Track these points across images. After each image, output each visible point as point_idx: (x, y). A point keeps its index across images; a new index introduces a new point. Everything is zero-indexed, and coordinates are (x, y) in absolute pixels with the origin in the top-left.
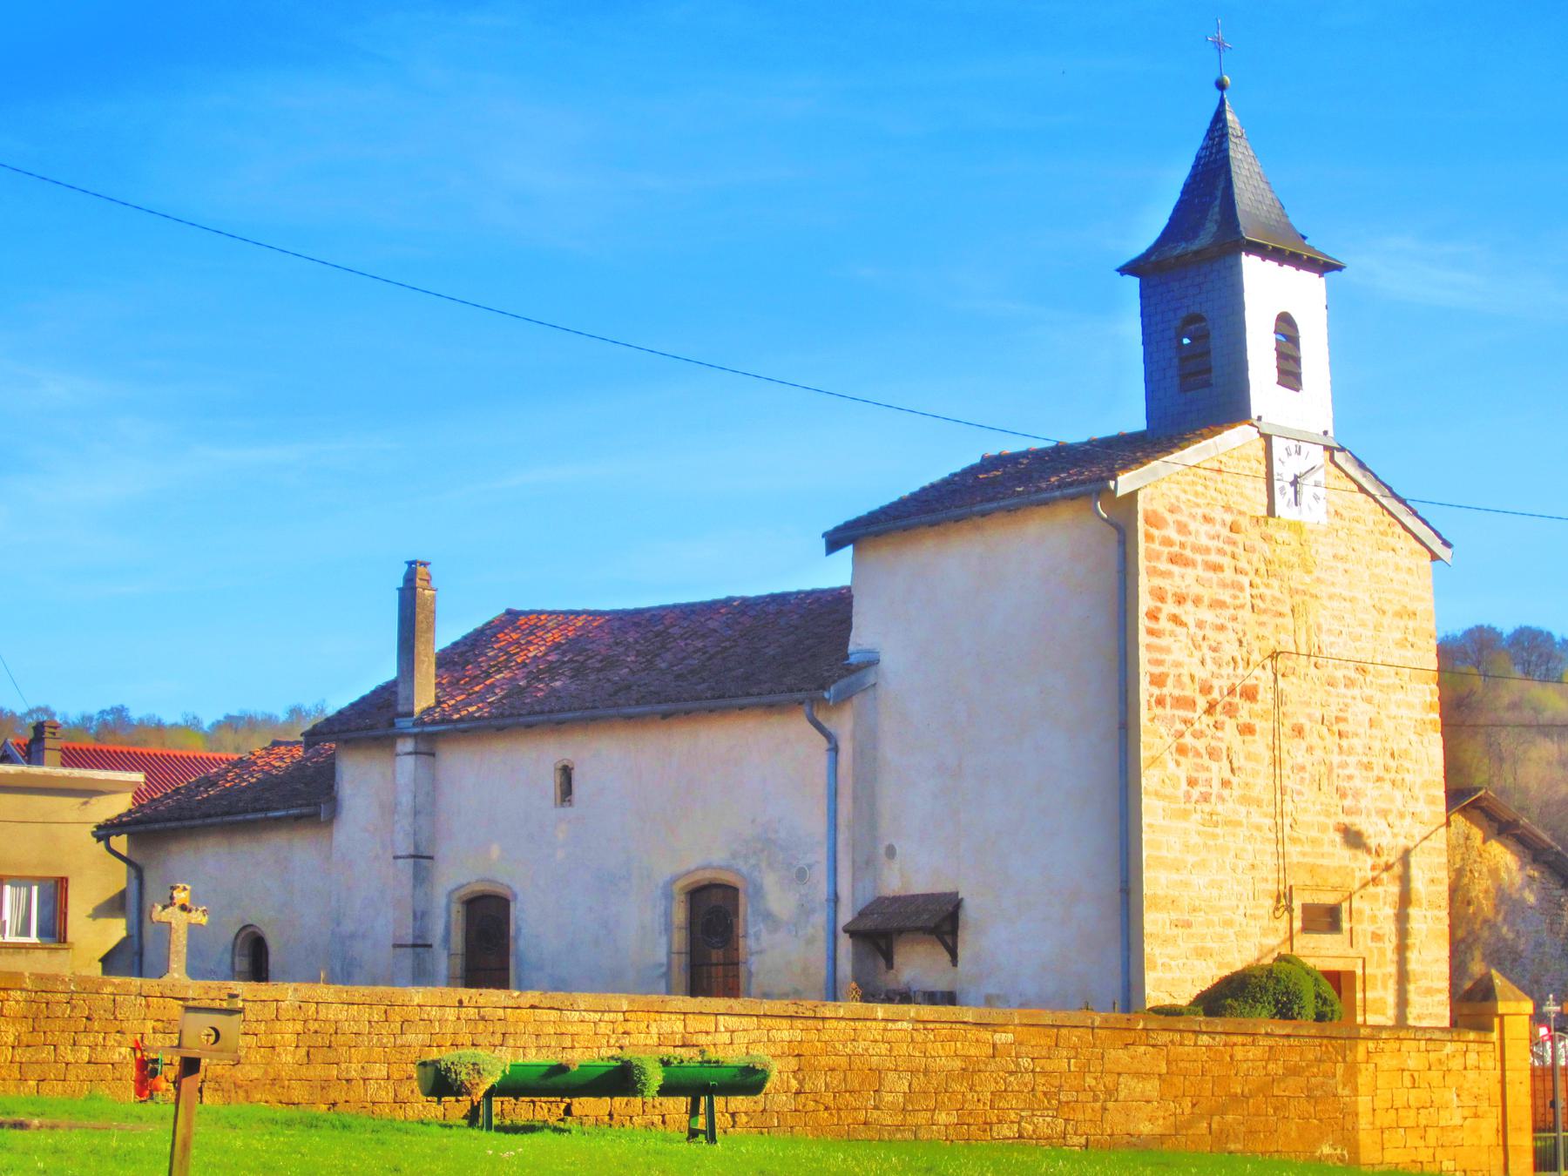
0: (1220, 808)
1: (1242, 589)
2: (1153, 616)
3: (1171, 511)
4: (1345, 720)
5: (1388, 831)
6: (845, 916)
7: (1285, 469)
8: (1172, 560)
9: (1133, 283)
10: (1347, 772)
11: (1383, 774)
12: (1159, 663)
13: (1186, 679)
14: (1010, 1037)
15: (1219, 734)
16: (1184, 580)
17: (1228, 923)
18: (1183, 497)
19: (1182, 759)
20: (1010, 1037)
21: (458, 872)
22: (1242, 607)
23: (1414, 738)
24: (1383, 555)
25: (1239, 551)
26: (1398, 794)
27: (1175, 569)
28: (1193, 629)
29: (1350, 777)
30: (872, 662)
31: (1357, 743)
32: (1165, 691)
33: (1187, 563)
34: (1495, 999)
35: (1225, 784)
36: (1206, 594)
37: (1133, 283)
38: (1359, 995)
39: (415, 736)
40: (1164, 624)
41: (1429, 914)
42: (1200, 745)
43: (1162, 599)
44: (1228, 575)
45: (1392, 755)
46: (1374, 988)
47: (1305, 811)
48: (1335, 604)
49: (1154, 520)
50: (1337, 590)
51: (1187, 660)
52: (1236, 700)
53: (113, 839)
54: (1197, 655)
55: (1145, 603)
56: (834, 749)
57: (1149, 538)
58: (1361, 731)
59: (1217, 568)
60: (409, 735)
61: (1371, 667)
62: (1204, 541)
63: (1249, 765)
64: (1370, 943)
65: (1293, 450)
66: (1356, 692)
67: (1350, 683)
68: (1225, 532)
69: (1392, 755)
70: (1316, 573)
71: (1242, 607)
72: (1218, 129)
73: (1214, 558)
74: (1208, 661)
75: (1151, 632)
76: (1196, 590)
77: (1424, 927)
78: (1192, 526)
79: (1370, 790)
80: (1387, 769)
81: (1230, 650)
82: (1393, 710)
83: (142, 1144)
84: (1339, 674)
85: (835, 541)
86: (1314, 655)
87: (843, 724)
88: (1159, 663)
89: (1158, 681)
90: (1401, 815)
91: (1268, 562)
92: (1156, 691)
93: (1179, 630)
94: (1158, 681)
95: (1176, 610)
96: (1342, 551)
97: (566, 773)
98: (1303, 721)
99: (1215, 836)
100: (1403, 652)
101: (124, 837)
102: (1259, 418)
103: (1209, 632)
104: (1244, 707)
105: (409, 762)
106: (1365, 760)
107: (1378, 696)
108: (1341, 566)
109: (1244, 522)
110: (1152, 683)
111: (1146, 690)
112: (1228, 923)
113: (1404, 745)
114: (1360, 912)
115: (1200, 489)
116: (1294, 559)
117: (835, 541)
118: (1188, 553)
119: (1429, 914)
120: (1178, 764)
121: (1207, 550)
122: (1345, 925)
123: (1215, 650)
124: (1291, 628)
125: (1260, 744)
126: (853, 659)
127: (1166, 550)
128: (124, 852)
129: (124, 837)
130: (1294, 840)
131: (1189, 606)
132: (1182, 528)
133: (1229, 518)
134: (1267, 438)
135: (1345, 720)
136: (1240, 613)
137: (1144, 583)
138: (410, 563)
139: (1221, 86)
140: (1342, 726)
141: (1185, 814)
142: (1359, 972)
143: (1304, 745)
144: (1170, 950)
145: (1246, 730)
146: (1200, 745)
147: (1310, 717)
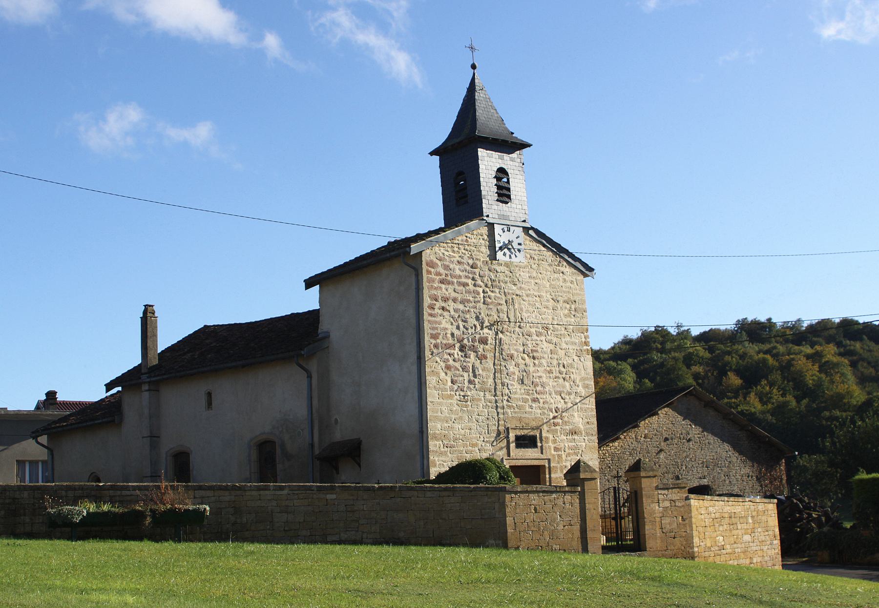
0: (469, 393)
1: (478, 294)
2: (432, 307)
3: (440, 260)
4: (536, 351)
5: (562, 401)
6: (317, 452)
7: (501, 238)
8: (442, 282)
9: (436, 158)
10: (539, 374)
11: (558, 375)
12: (433, 329)
13: (449, 336)
14: (334, 496)
15: (468, 359)
16: (447, 291)
17: (473, 445)
18: (446, 253)
19: (448, 372)
20: (334, 496)
21: (168, 444)
22: (479, 302)
23: (576, 358)
24: (556, 275)
25: (477, 277)
26: (567, 384)
27: (443, 286)
28: (452, 313)
29: (540, 377)
30: (327, 336)
31: (544, 361)
32: (439, 341)
33: (449, 283)
34: (579, 472)
35: (470, 382)
36: (459, 297)
37: (436, 158)
38: (547, 476)
39: (149, 382)
40: (437, 311)
41: (586, 438)
42: (457, 365)
43: (436, 300)
44: (471, 287)
45: (564, 366)
46: (556, 472)
47: (516, 393)
48: (530, 299)
49: (431, 264)
50: (532, 292)
51: (450, 327)
52: (476, 344)
53: (39, 439)
54: (455, 324)
55: (427, 301)
56: (310, 377)
57: (429, 272)
58: (546, 356)
59: (465, 285)
60: (145, 383)
61: (551, 326)
62: (458, 272)
63: (484, 374)
64: (553, 452)
65: (506, 229)
66: (543, 338)
67: (539, 334)
68: (468, 268)
69: (564, 366)
70: (519, 285)
71: (479, 302)
72: (472, 88)
73: (463, 280)
74: (461, 327)
75: (431, 315)
76: (454, 295)
77: (584, 444)
78: (451, 266)
79: (551, 382)
80: (560, 373)
81: (472, 321)
82: (564, 346)
83: (58, 583)
84: (533, 330)
85: (309, 283)
86: (520, 323)
87: (313, 366)
88: (433, 329)
89: (435, 337)
90: (570, 394)
91: (493, 281)
92: (433, 341)
93: (445, 313)
94: (435, 337)
95: (443, 304)
96: (534, 274)
97: (209, 395)
98: (512, 352)
99: (466, 406)
100: (568, 319)
101: (45, 437)
102: (488, 216)
103: (461, 314)
104: (480, 348)
105: (146, 394)
106: (548, 369)
107: (555, 340)
108: (533, 281)
109: (479, 264)
110: (431, 338)
111: (428, 342)
112: (473, 445)
113: (570, 361)
114: (547, 438)
115: (456, 249)
116: (507, 279)
117: (309, 283)
118: (449, 278)
119: (586, 438)
120: (446, 374)
121: (460, 277)
122: (539, 444)
123: (465, 322)
124: (505, 310)
125: (489, 364)
126: (320, 336)
127: (438, 278)
128: (46, 444)
129: (45, 437)
130: (509, 407)
131: (451, 303)
132: (446, 267)
133: (471, 262)
134: (491, 226)
135: (536, 351)
136: (478, 305)
137: (426, 294)
138: (145, 306)
139: (474, 67)
140: (535, 354)
141: (450, 397)
142: (547, 465)
143: (514, 363)
144: (443, 458)
145: (482, 358)
146: (457, 365)
147: (517, 350)
